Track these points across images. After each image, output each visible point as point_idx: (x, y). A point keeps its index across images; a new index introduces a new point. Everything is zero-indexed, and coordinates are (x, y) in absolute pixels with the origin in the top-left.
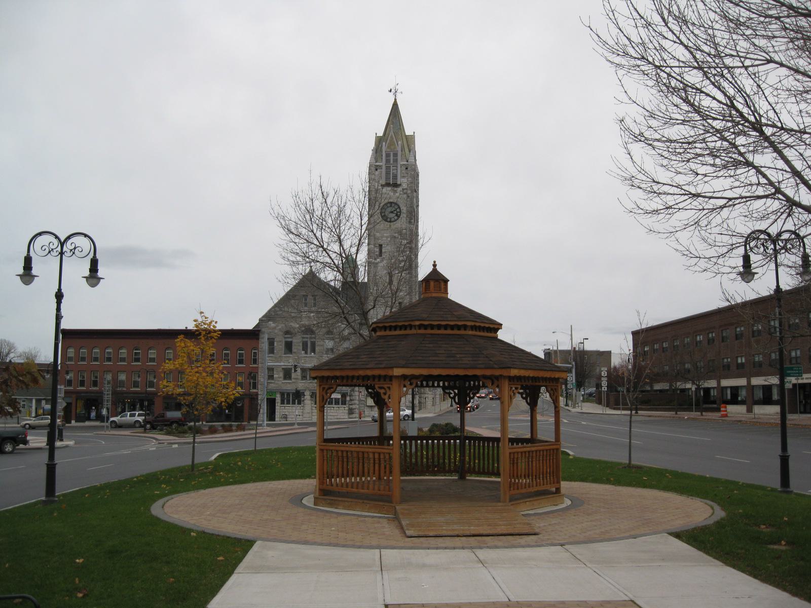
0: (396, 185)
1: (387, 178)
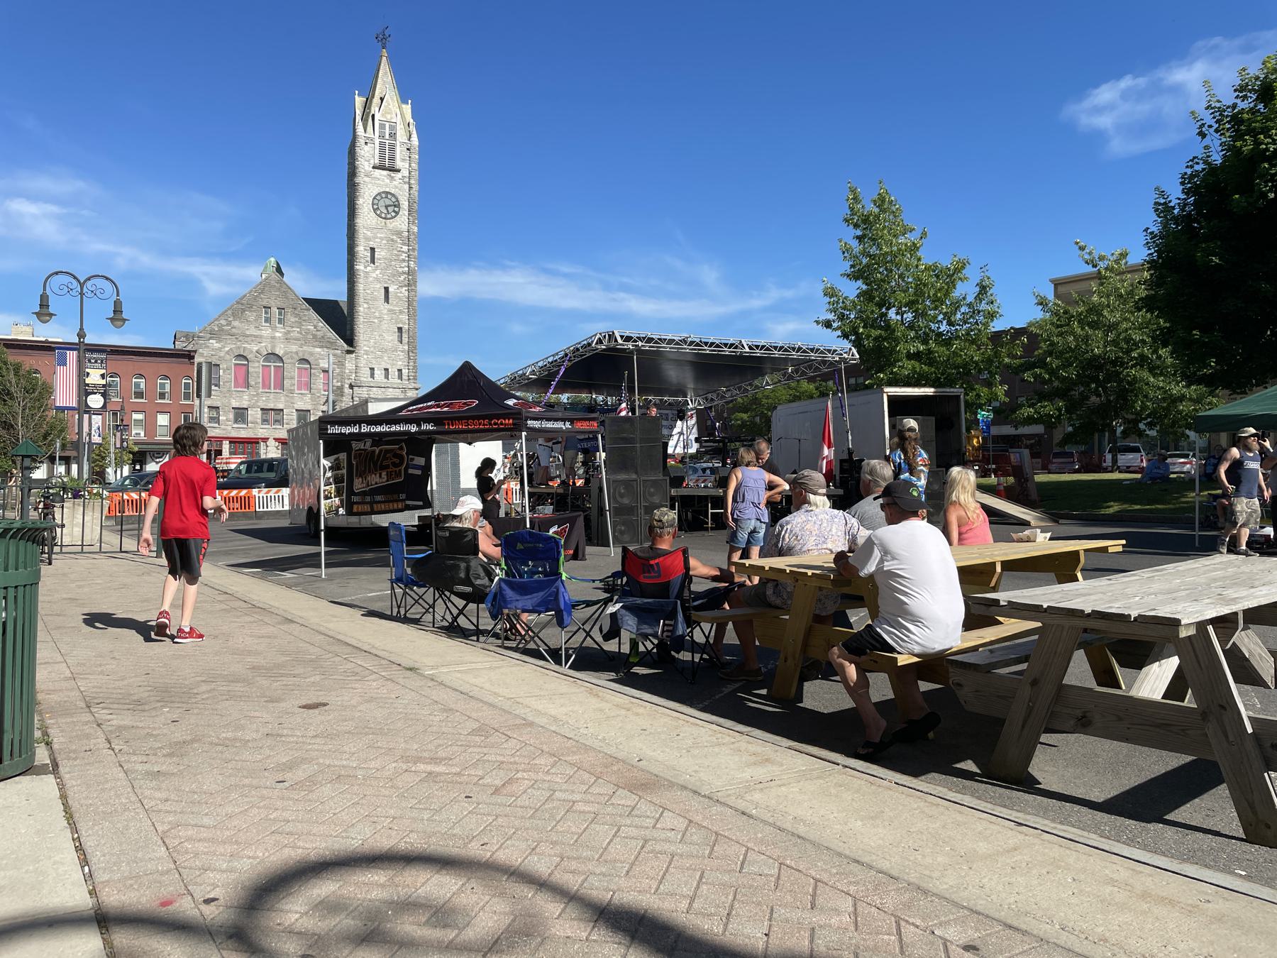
0: (394, 170)
1: (382, 157)
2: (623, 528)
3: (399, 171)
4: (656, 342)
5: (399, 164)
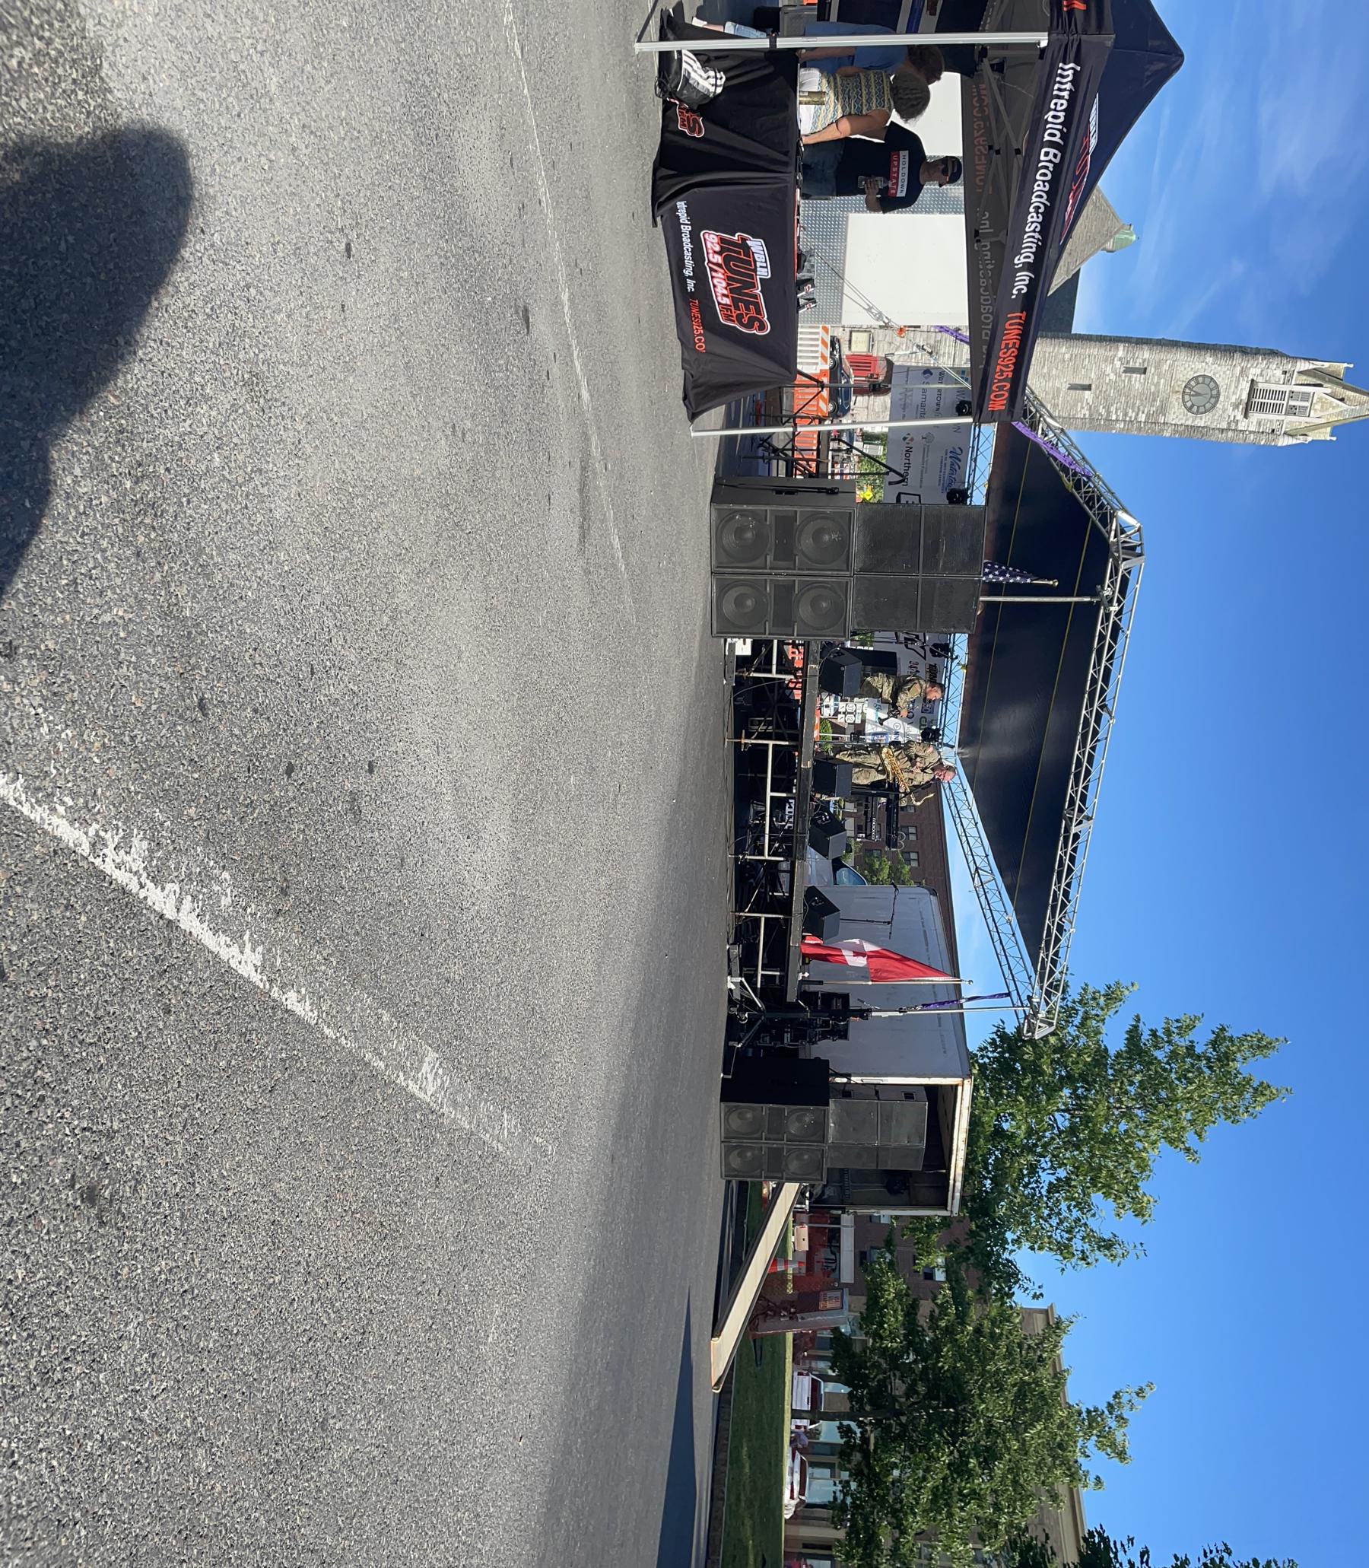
1: (1265, 393)
2: (749, 535)
3: (1246, 416)
4: (1111, 647)
5: (1255, 417)
